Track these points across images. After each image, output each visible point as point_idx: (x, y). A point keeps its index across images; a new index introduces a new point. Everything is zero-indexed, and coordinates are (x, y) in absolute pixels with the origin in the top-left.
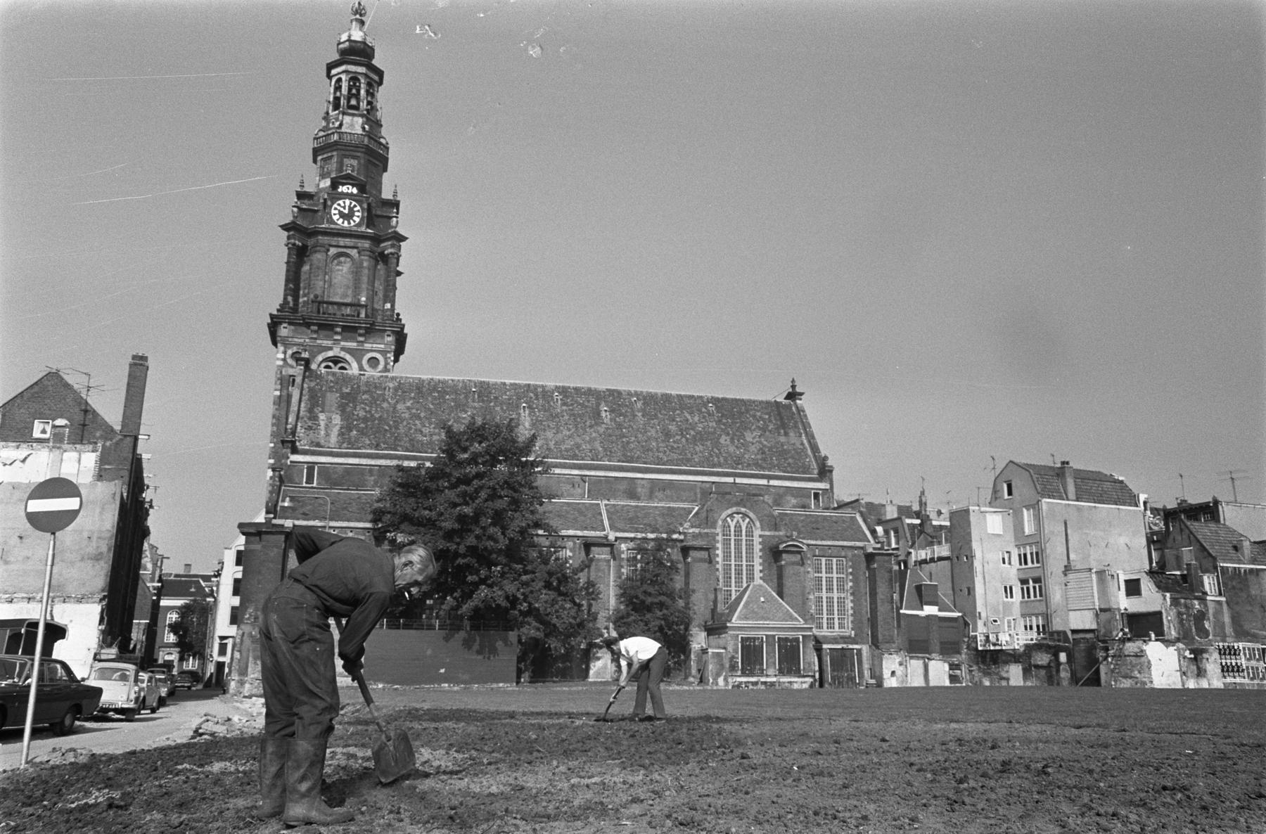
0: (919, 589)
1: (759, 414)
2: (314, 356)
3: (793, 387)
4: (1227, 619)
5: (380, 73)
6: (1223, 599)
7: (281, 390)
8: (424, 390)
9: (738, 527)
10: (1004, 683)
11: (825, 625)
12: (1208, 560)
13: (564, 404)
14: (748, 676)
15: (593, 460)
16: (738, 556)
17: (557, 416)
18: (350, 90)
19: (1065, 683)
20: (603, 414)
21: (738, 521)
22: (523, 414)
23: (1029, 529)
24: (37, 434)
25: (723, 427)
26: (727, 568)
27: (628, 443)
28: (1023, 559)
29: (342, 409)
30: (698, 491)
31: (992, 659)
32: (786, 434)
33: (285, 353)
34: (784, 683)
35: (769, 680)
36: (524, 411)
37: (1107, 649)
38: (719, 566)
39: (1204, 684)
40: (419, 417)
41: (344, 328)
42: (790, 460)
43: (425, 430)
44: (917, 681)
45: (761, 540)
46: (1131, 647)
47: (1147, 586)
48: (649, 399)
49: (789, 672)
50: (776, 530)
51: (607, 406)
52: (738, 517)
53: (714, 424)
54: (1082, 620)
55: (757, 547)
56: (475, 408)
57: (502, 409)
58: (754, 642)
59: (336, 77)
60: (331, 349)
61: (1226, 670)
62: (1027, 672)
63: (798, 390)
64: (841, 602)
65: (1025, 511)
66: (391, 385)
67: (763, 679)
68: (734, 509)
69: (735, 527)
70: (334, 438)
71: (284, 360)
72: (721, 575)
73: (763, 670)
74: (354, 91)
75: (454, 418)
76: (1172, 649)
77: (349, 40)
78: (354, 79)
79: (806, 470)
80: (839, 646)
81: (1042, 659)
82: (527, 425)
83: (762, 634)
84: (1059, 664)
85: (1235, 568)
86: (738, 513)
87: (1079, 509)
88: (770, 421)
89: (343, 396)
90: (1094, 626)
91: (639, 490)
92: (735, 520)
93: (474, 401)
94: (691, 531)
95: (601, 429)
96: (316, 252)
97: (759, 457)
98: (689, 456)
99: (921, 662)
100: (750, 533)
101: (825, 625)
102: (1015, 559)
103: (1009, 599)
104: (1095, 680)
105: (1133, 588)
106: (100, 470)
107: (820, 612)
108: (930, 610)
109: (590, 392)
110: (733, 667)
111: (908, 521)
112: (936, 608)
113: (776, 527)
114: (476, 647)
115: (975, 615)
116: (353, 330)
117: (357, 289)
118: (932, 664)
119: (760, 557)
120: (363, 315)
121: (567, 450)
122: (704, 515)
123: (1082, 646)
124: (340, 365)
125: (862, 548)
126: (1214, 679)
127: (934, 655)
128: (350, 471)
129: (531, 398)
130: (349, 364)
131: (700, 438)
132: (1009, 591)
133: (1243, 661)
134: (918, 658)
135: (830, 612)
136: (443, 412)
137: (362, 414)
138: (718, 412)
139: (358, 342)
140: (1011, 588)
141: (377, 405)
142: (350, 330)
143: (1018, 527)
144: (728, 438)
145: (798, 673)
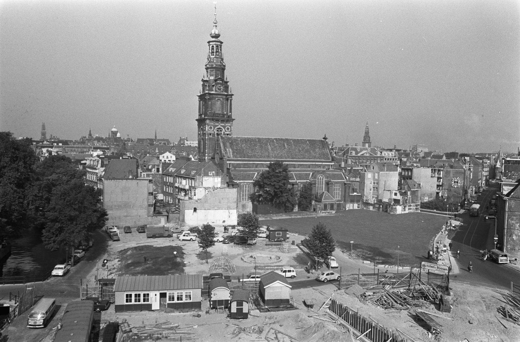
0: (353, 189)
2: (214, 128)
3: (325, 136)
4: (411, 200)
5: (222, 43)
6: (411, 196)
9: (320, 178)
10: (368, 209)
12: (409, 189)
13: (277, 143)
16: (320, 185)
18: (216, 50)
19: (381, 211)
20: (286, 146)
23: (376, 178)
24: (209, 175)
26: (318, 187)
28: (374, 183)
29: (231, 146)
31: (367, 204)
33: (208, 127)
37: (390, 206)
39: (405, 212)
40: (247, 148)
41: (221, 121)
43: (250, 152)
44: (351, 208)
46: (394, 207)
47: (398, 194)
48: (294, 141)
52: (320, 176)
53: (309, 147)
54: (386, 200)
55: (324, 182)
60: (218, 126)
61: (409, 209)
62: (374, 208)
65: (376, 174)
70: (232, 156)
71: (208, 129)
72: (317, 188)
74: (217, 50)
76: (401, 207)
77: (215, 34)
78: (217, 46)
81: (377, 206)
82: (270, 149)
83: (327, 203)
84: (380, 207)
87: (386, 173)
89: (230, 143)
90: (388, 202)
96: (213, 99)
100: (323, 179)
102: (373, 183)
104: (387, 211)
105: (396, 194)
106: (221, 181)
107: (335, 195)
108: (355, 194)
109: (282, 139)
110: (322, 209)
111: (348, 168)
113: (328, 178)
114: (277, 208)
115: (364, 195)
116: (223, 121)
117: (223, 109)
118: (354, 204)
120: (225, 117)
121: (280, 156)
123: (385, 205)
125: (344, 182)
126: (407, 211)
128: (238, 164)
131: (307, 151)
132: (371, 190)
133: (412, 207)
135: (336, 195)
137: (235, 148)
142: (223, 121)
143: (374, 177)
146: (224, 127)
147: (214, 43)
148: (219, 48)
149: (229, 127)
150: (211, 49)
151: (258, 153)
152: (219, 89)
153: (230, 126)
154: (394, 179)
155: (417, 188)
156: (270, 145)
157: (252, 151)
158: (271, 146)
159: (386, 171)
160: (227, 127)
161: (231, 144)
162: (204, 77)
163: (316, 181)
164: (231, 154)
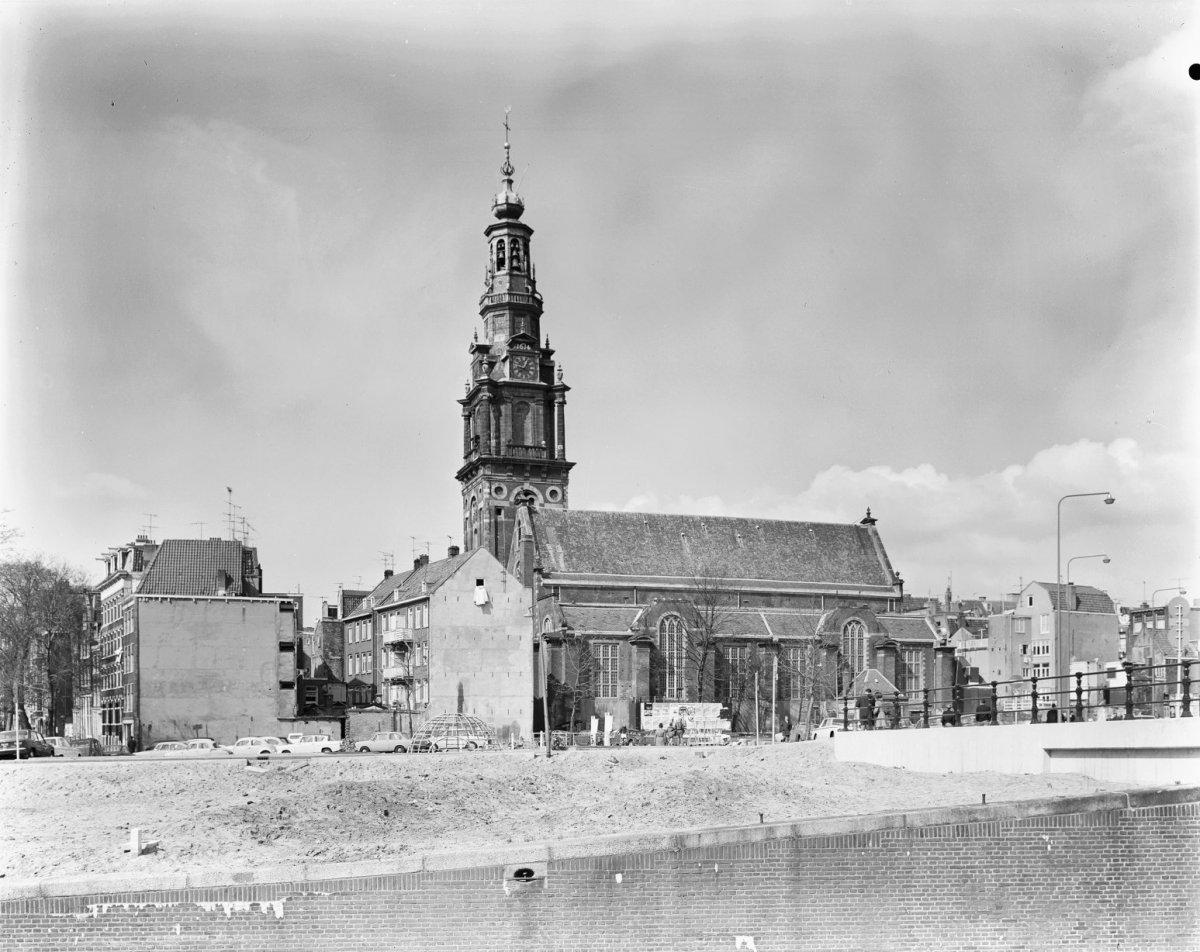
3: (869, 514)
7: (490, 519)
18: (512, 252)
20: (738, 540)
29: (560, 538)
32: (866, 553)
40: (611, 545)
53: (815, 546)
55: (865, 644)
59: (499, 239)
63: (872, 516)
68: (851, 618)
70: (562, 565)
71: (490, 494)
74: (514, 253)
78: (514, 242)
79: (883, 581)
89: (559, 529)
95: (739, 551)
113: (878, 630)
130: (535, 495)
147: (505, 231)
148: (521, 247)
150: (495, 250)
151: (648, 558)
152: (522, 370)
157: (628, 553)
158: (689, 540)
161: (562, 531)
162: (476, 338)
164: (561, 560)
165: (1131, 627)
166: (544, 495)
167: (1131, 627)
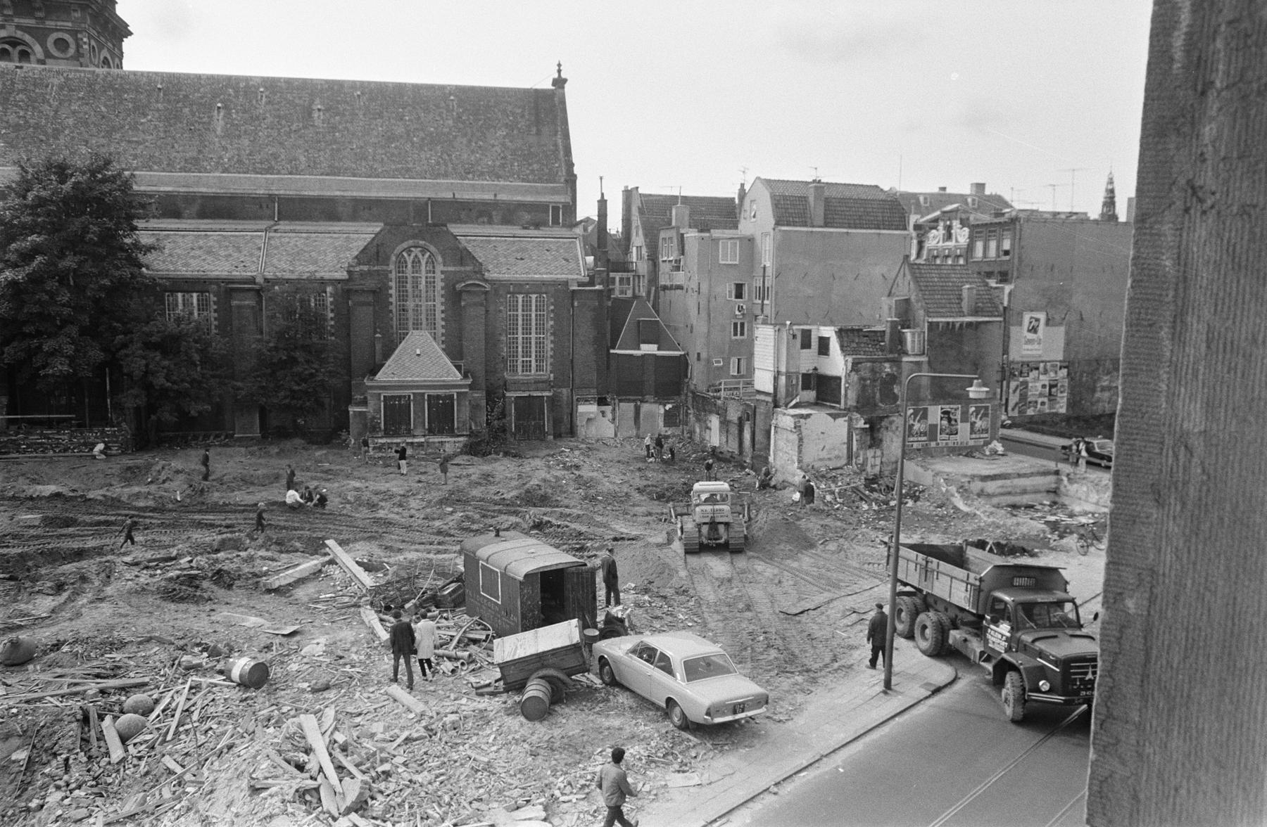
1: (510, 108)
3: (559, 71)
6: (924, 359)
8: (97, 87)
11: (520, 369)
14: (392, 436)
15: (290, 173)
17: (257, 118)
20: (316, 115)
21: (416, 256)
22: (216, 117)
25: (461, 126)
27: (338, 150)
30: (411, 208)
34: (434, 443)
35: (416, 440)
36: (219, 112)
38: (393, 308)
42: (535, 166)
45: (443, 276)
49: (441, 432)
50: (462, 265)
51: (322, 103)
52: (416, 251)
53: (450, 122)
55: (439, 285)
56: (158, 110)
57: (191, 111)
58: (400, 401)
63: (563, 75)
64: (539, 343)
66: (56, 81)
67: (409, 440)
68: (411, 242)
69: (413, 262)
73: (410, 430)
75: (129, 124)
76: (842, 423)
80: (526, 394)
85: (948, 323)
86: (416, 247)
88: (523, 116)
91: (340, 209)
92: (413, 255)
93: (157, 102)
94: (357, 269)
95: (310, 133)
97: (498, 163)
98: (411, 165)
99: (632, 405)
101: (520, 369)
103: (738, 337)
108: (649, 349)
112: (655, 346)
113: (461, 262)
118: (645, 408)
119: (442, 296)
122: (375, 250)
124: (20, 48)
125: (566, 283)
127: (647, 397)
129: (230, 95)
130: (31, 48)
134: (629, 401)
135: (527, 353)
136: (117, 116)
138: (459, 106)
139: (36, 18)
140: (742, 325)
141: (34, 108)
144: (465, 141)
145: (451, 432)
146: (40, 35)
149: (66, 37)
153: (74, 33)
154: (878, 271)
155: (976, 312)
156: (226, 107)
159: (826, 225)
160: (55, 36)
163: (386, 274)
165: (970, 248)
166: (43, 45)
167: (970, 248)
